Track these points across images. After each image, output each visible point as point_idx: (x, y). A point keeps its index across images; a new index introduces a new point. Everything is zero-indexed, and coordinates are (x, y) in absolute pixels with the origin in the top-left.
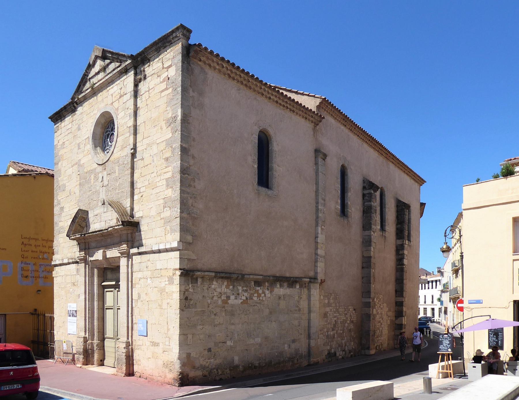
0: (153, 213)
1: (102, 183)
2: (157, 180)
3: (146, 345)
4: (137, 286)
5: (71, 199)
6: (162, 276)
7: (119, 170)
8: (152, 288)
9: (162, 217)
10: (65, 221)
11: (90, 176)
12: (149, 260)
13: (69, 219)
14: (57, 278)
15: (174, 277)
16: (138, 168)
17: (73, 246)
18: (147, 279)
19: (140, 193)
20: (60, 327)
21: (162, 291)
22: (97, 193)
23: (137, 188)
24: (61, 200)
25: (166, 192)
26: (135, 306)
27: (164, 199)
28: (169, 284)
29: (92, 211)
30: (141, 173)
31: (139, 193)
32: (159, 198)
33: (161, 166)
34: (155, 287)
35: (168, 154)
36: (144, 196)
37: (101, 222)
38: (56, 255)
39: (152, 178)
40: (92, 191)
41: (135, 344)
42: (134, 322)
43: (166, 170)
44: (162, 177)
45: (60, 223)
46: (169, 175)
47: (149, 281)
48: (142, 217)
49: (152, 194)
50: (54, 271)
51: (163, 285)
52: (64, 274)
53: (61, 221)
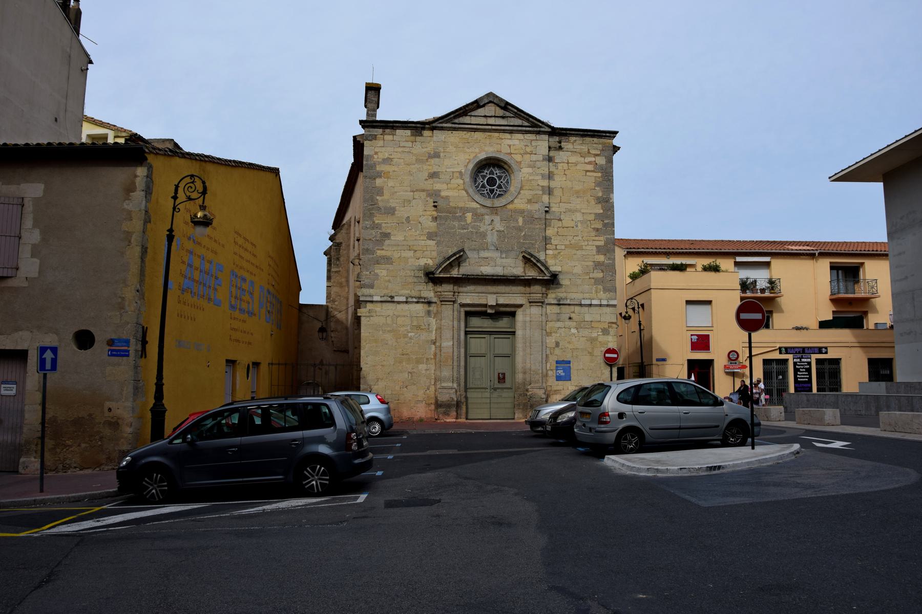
0: (578, 270)
1: (490, 227)
2: (583, 244)
3: (568, 389)
4: (553, 334)
5: (410, 228)
6: (592, 327)
7: (524, 221)
8: (577, 338)
9: (591, 275)
10: (394, 251)
11: (464, 214)
12: (573, 312)
13: (404, 250)
14: (371, 318)
15: (610, 329)
16: (552, 226)
17: (415, 283)
18: (570, 329)
19: (556, 249)
20: (378, 379)
21: (593, 340)
22: (483, 235)
23: (551, 244)
24: (383, 225)
25: (597, 257)
26: (551, 354)
27: (594, 262)
28: (604, 334)
29: (475, 252)
30: (558, 232)
31: (554, 249)
32: (586, 260)
33: (588, 233)
34: (582, 337)
35: (599, 225)
36: (562, 253)
37: (495, 266)
38: (368, 290)
39: (575, 240)
40: (469, 231)
41: (551, 390)
42: (548, 368)
43: (597, 238)
44: (590, 243)
45: (378, 252)
46: (602, 243)
47: (574, 331)
48: (560, 272)
49: (575, 254)
50: (360, 308)
51: (594, 335)
52: (391, 315)
53: (383, 249)
